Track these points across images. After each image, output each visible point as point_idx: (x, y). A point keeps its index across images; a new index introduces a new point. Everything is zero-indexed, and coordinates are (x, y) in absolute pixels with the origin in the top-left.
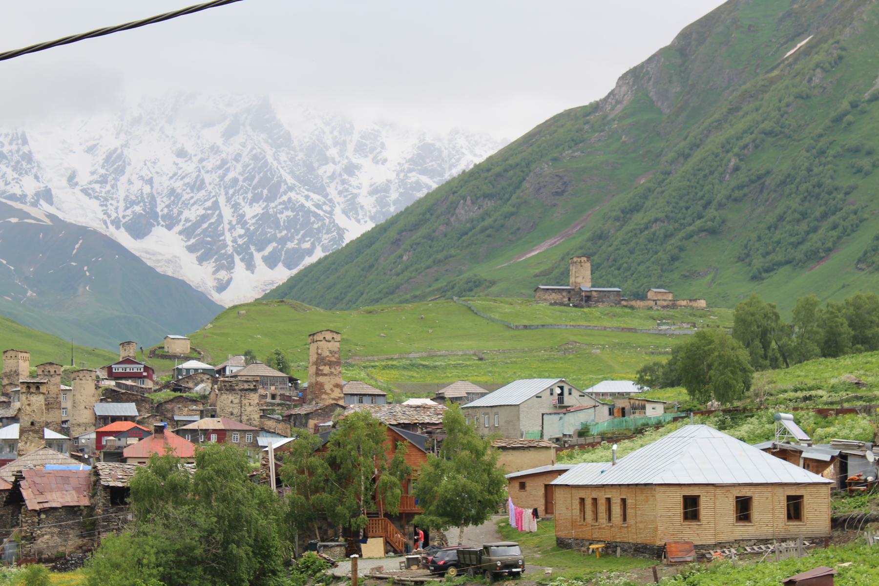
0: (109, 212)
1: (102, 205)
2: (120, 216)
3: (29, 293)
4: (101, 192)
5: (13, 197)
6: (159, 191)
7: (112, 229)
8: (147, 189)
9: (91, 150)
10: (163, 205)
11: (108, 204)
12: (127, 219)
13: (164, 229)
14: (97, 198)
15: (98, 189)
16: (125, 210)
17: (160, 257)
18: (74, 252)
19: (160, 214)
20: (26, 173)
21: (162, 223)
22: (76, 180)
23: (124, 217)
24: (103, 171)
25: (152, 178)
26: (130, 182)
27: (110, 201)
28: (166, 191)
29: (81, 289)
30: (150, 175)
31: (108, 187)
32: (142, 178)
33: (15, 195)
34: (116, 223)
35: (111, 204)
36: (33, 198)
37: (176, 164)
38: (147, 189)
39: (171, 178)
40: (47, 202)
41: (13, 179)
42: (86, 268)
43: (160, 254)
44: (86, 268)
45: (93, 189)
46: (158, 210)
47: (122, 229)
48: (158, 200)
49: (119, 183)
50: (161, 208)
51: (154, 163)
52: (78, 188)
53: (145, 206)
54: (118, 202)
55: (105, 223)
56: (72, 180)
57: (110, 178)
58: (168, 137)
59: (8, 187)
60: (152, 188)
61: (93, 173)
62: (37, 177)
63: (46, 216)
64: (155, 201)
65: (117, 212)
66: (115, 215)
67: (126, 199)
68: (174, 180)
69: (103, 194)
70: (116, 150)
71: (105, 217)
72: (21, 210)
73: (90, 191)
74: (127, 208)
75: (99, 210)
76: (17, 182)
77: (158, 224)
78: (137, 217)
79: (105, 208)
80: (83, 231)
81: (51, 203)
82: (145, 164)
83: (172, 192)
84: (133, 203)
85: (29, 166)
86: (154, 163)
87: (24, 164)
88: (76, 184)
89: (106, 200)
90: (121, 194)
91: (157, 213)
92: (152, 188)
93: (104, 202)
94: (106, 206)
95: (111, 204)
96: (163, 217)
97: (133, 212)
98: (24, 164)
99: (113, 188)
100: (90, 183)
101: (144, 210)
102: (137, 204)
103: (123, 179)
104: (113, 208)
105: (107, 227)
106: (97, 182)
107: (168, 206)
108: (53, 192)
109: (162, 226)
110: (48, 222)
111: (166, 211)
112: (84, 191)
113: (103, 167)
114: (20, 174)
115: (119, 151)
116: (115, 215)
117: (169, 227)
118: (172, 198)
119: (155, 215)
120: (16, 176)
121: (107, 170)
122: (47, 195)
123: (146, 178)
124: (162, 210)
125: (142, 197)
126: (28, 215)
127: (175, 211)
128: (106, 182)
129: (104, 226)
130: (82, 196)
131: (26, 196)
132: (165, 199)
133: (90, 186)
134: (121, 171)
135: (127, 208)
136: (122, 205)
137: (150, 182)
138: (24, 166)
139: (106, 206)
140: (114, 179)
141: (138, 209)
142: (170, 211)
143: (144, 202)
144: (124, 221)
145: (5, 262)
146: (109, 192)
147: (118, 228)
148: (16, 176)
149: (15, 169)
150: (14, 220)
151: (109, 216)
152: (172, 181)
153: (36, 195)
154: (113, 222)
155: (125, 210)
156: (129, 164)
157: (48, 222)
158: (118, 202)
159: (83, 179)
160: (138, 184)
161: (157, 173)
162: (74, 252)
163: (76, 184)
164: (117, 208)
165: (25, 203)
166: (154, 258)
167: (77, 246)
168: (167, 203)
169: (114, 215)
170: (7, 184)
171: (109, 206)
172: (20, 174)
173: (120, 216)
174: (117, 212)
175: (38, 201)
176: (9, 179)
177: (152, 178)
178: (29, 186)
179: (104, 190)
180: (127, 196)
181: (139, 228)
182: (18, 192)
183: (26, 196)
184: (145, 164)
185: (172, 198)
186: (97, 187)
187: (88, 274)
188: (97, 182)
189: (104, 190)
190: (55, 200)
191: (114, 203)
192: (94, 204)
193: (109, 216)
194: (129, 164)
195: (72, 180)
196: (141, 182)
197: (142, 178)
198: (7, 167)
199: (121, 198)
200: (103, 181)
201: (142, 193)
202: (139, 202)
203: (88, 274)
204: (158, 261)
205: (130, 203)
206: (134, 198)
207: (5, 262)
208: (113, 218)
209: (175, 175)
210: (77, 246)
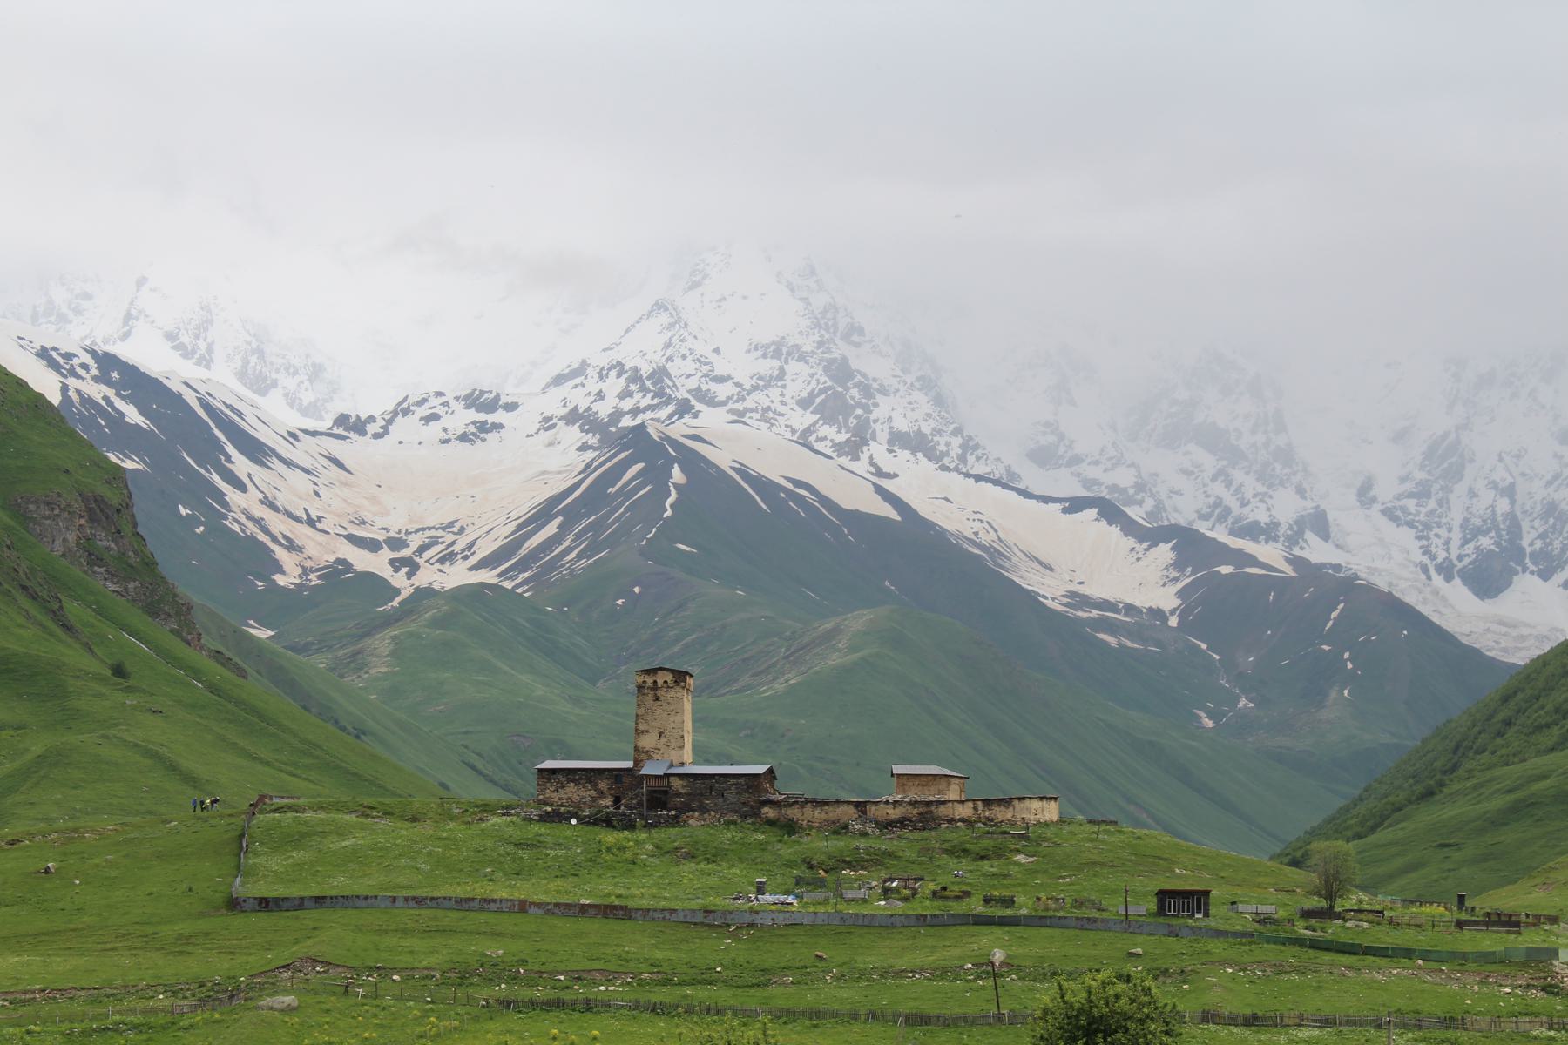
0: (1433, 549)
1: (1419, 538)
2: (1454, 557)
3: (1243, 702)
4: (1418, 513)
5: (1253, 531)
6: (1527, 508)
7: (1438, 580)
8: (1503, 505)
9: (1400, 437)
10: (1534, 534)
11: (1432, 534)
12: (1467, 561)
13: (1536, 579)
14: (1410, 524)
15: (1412, 509)
16: (1462, 545)
17: (1525, 631)
18: (1330, 624)
19: (1528, 550)
20: (1282, 484)
21: (1532, 567)
22: (1372, 493)
23: (1460, 558)
24: (1420, 475)
25: (1512, 485)
26: (1473, 494)
27: (1436, 530)
28: (1539, 507)
29: (1333, 694)
30: (1510, 480)
31: (1432, 504)
32: (1494, 485)
33: (1257, 523)
34: (1446, 570)
35: (1437, 535)
36: (1291, 528)
37: (1556, 456)
38: (1503, 505)
39: (1549, 483)
40: (1318, 534)
41: (1255, 496)
42: (1347, 655)
43: (1527, 625)
44: (1347, 655)
45: (1404, 510)
46: (1525, 543)
47: (1457, 581)
48: (1525, 525)
49: (1452, 497)
50: (1529, 540)
51: (1518, 457)
52: (1377, 507)
53: (1499, 536)
54: (1450, 530)
55: (1425, 570)
56: (1365, 494)
57: (1436, 487)
58: (1543, 407)
59: (1246, 510)
60: (1513, 502)
61: (1403, 479)
62: (1301, 492)
63: (1287, 559)
64: (1519, 527)
65: (1447, 550)
66: (1444, 554)
67: (1464, 525)
68: (1553, 488)
69: (1422, 518)
70: (1446, 435)
71: (1425, 560)
72: (1239, 552)
73: (1399, 513)
74: (1465, 542)
75: (1415, 547)
76: (1262, 501)
77: (1524, 571)
78: (1484, 556)
79: (1425, 542)
80: (1346, 587)
81: (1326, 537)
82: (1501, 460)
83: (1551, 509)
84: (1477, 532)
85: (1287, 470)
86: (1518, 457)
87: (1278, 466)
88: (1374, 500)
89: (1427, 527)
90: (1456, 517)
91: (1521, 550)
92: (1513, 502)
93: (1424, 531)
94: (1428, 538)
95: (1437, 535)
96: (1533, 555)
97: (1477, 548)
98: (1278, 466)
99: (1441, 506)
100: (1399, 497)
101: (1497, 544)
102: (1485, 533)
103: (1460, 489)
104: (1439, 542)
105: (1429, 578)
106: (1411, 495)
107: (1542, 536)
108: (1330, 516)
109: (1532, 573)
110: (1289, 571)
111: (1538, 545)
112: (1388, 513)
113: (1422, 467)
114: (1270, 486)
115: (1453, 436)
116: (1444, 554)
117: (1545, 575)
118: (1551, 521)
119: (1517, 553)
120: (1261, 489)
121: (1429, 473)
122: (1319, 523)
123: (1502, 485)
124: (1531, 544)
125: (1494, 520)
126: (1252, 560)
127: (1557, 544)
128: (1428, 495)
129: (1423, 577)
130: (1383, 522)
131: (1277, 525)
132: (1537, 523)
133: (1398, 503)
134: (1455, 474)
135: (1465, 542)
136: (1456, 537)
137: (1510, 492)
138: (1278, 471)
139: (1428, 538)
140: (1442, 489)
141: (1486, 542)
142: (1547, 545)
143: (1498, 530)
144: (1460, 565)
145: (1204, 646)
146: (1432, 512)
147: (1448, 579)
148: (1264, 489)
149: (1260, 477)
150: (1225, 570)
151: (1433, 558)
152: (1551, 489)
153: (1296, 522)
154: (1439, 569)
155: (1462, 545)
156: (1472, 461)
157: (1289, 571)
158: (1450, 530)
159: (1386, 491)
160: (1487, 497)
161: (1523, 474)
162: (1330, 624)
163: (1374, 500)
164: (1447, 542)
165: (1276, 539)
166: (1514, 633)
167: (1334, 615)
168: (1541, 530)
169: (1441, 555)
170: (1244, 504)
171: (1435, 540)
172: (1270, 486)
173: (1454, 557)
174: (1447, 550)
175: (1300, 533)
176: (1249, 494)
177: (1512, 485)
178: (1286, 508)
179: (1424, 510)
180: (1466, 520)
181: (1487, 579)
182: (1263, 518)
183: (1277, 525)
184: (1501, 460)
185: (1551, 521)
186: (1411, 504)
187: (1350, 666)
188: (1411, 495)
189: (1424, 510)
190: (1333, 530)
191: (1443, 532)
192: (1406, 536)
193: (1433, 558)
194: (1472, 461)
195: (1365, 494)
196: (1493, 493)
197: (1494, 485)
198: (1247, 473)
199: (1456, 524)
200: (1422, 493)
201: (1494, 512)
202: (1489, 530)
203: (1350, 666)
204: (1522, 638)
205: (1471, 533)
206: (1478, 522)
207: (1204, 646)
208: (1439, 560)
209: (1556, 477)
210: (1334, 615)
